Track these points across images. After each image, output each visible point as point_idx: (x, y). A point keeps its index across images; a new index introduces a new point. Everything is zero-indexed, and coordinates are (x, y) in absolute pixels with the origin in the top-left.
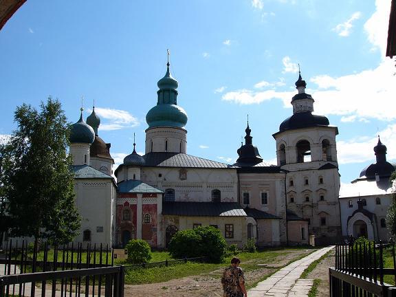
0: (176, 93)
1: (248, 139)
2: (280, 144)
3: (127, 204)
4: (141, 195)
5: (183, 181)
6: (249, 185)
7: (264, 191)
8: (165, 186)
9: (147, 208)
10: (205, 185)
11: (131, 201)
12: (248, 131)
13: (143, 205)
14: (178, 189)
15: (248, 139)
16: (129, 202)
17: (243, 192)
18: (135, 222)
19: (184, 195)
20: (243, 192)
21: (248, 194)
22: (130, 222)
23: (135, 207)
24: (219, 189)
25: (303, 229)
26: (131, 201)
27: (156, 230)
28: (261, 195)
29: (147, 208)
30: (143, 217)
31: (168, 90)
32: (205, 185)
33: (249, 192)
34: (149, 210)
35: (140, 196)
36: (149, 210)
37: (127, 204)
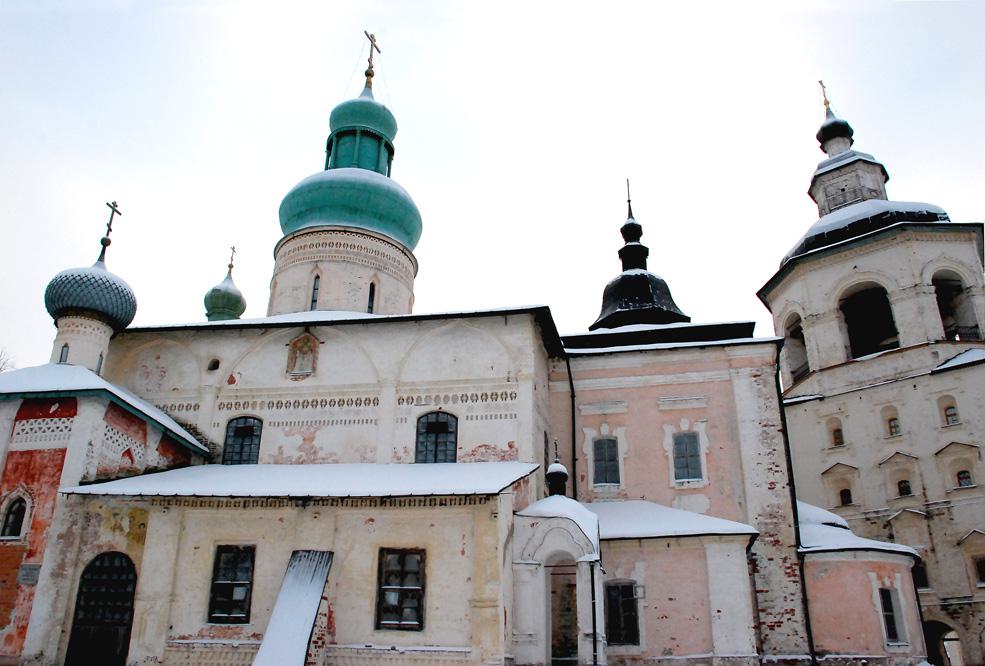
0: (391, 151)
1: (634, 255)
2: (785, 316)
5: (308, 382)
6: (617, 402)
7: (685, 427)
8: (229, 406)
10: (388, 397)
12: (632, 231)
14: (282, 414)
15: (634, 255)
17: (587, 438)
19: (298, 440)
20: (587, 438)
21: (612, 443)
24: (447, 407)
25: (886, 595)
28: (669, 444)
32: (388, 397)
33: (620, 434)
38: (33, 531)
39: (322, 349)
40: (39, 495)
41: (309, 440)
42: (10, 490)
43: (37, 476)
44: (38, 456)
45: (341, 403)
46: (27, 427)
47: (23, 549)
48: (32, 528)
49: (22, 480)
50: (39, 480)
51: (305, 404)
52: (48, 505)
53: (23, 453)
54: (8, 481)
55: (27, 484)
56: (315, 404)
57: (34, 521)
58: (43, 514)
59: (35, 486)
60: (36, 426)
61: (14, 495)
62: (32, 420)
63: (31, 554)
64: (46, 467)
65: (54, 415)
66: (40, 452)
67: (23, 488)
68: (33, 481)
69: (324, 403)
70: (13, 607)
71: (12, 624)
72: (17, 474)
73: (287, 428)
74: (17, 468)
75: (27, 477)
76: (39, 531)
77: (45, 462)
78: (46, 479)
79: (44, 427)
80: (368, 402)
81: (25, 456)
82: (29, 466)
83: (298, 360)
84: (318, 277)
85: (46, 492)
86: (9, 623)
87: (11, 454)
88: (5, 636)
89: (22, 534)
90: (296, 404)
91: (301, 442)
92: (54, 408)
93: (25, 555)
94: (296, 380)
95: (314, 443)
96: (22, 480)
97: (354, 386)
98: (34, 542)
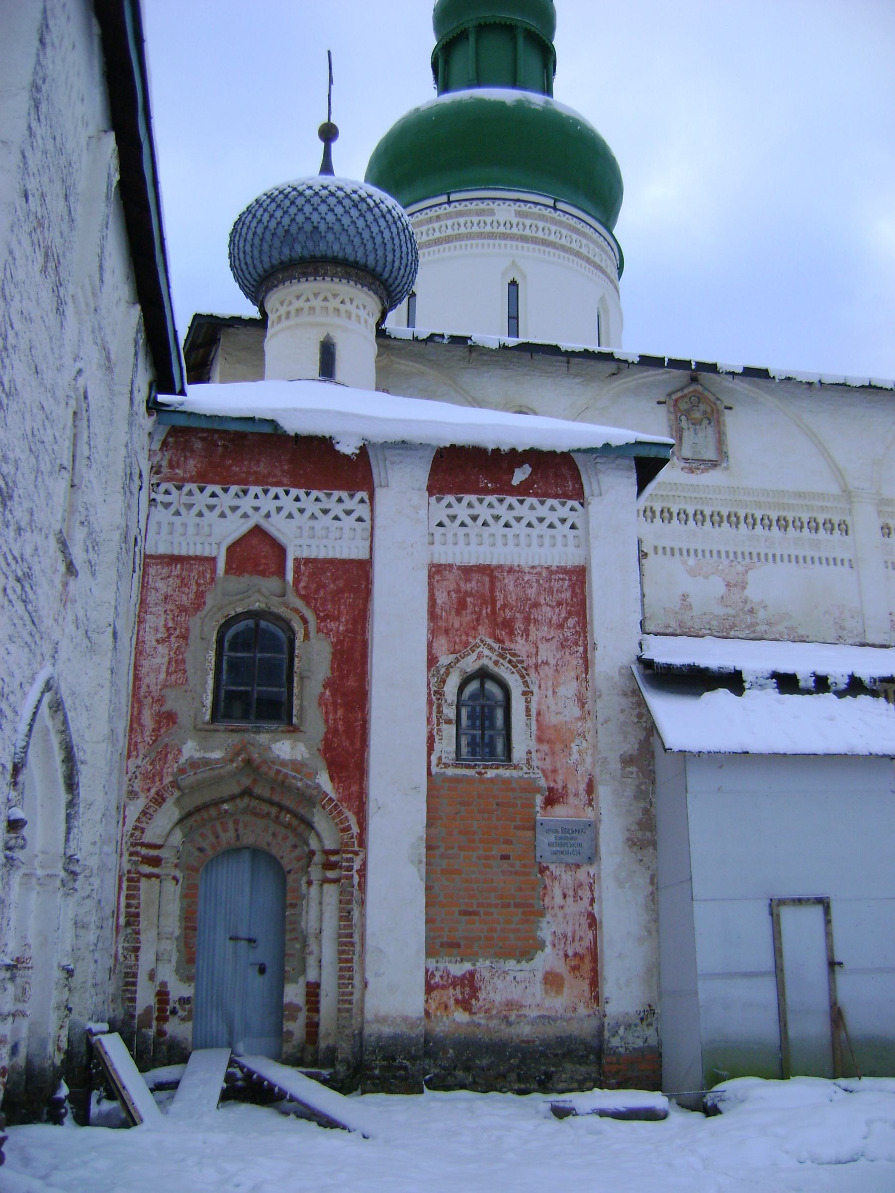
3: (257, 551)
4: (421, 473)
9: (472, 601)
10: (865, 521)
11: (310, 526)
13: (436, 571)
16: (281, 528)
18: (348, 756)
22: (286, 749)
23: (348, 584)
26: (310, 526)
27: (581, 845)
29: (472, 601)
30: (435, 696)
31: (509, 29)
34: (502, 629)
35: (402, 491)
36: (502, 629)
37: (257, 551)
38: (545, 747)
39: (729, 418)
40: (536, 667)
41: (737, 585)
42: (460, 650)
43: (519, 625)
44: (509, 581)
45: (783, 523)
46: (462, 512)
47: (530, 788)
48: (540, 740)
49: (483, 631)
50: (526, 633)
51: (717, 519)
52: (569, 689)
53: (467, 571)
54: (447, 632)
55: (499, 641)
56: (733, 520)
57: (540, 727)
58: (561, 706)
59: (520, 646)
60: (484, 513)
61: (470, 664)
62: (472, 498)
63: (552, 798)
64: (536, 605)
65: (523, 490)
66: (511, 570)
67: (491, 649)
68: (511, 633)
69: (752, 522)
70: (541, 913)
71: (548, 949)
72: (467, 617)
73: (691, 561)
74: (461, 606)
75: (494, 625)
76: (558, 747)
77: (532, 592)
78: (544, 631)
79: (484, 513)
80: (830, 526)
81: (475, 576)
82: (494, 602)
83: (686, 434)
84: (513, 284)
85: (552, 662)
86: (541, 946)
87: (436, 571)
88: (540, 976)
89: (518, 753)
90: (700, 517)
91: (723, 589)
92: (520, 475)
93: (539, 799)
94: (691, 471)
95: (747, 592)
96: (483, 631)
97: (800, 495)
98: (554, 771)
